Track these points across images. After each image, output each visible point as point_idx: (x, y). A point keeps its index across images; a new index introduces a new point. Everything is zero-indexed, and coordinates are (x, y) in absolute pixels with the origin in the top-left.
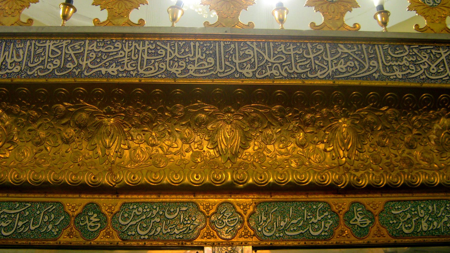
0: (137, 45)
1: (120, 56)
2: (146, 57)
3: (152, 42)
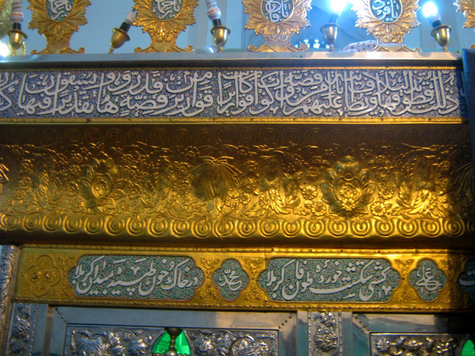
0: (340, 75)
1: (322, 90)
2: (353, 91)
3: (357, 72)
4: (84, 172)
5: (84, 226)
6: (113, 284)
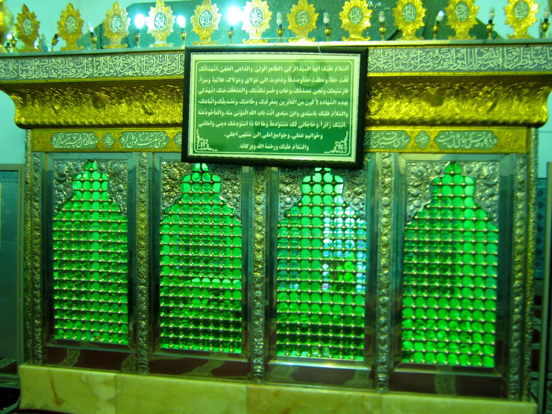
1: (133, 65)
2: (145, 65)
4: (51, 99)
5: (54, 122)
6: (67, 144)
